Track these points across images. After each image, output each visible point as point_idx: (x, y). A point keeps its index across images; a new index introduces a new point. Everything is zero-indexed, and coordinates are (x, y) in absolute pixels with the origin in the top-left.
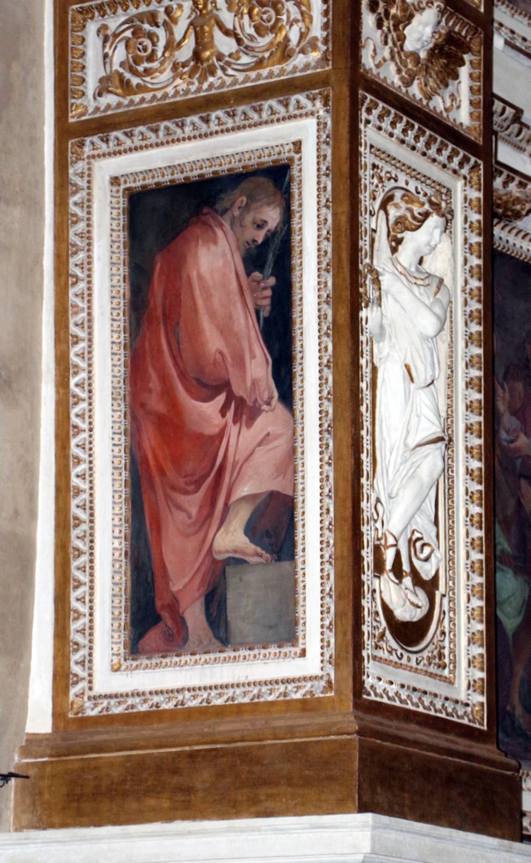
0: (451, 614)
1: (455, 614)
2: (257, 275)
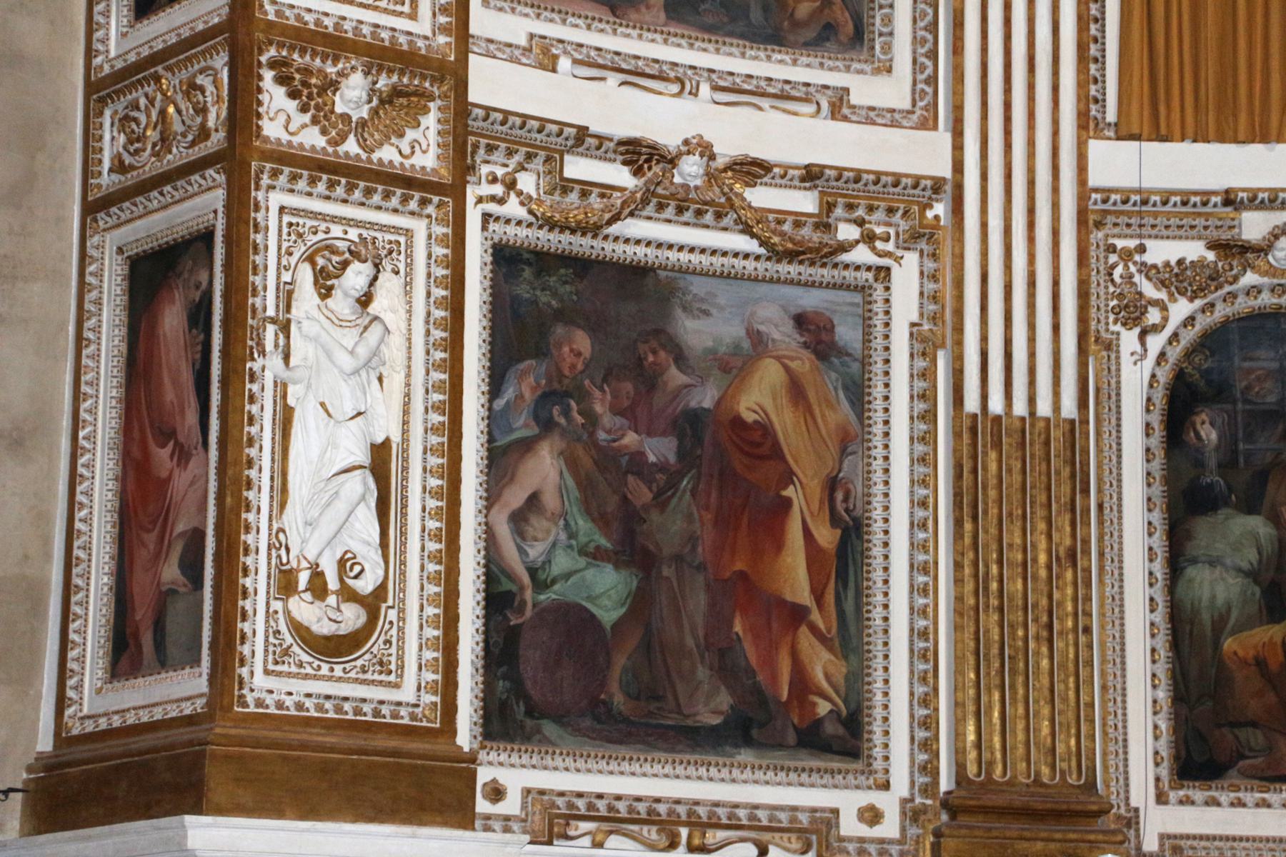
2: (194, 331)
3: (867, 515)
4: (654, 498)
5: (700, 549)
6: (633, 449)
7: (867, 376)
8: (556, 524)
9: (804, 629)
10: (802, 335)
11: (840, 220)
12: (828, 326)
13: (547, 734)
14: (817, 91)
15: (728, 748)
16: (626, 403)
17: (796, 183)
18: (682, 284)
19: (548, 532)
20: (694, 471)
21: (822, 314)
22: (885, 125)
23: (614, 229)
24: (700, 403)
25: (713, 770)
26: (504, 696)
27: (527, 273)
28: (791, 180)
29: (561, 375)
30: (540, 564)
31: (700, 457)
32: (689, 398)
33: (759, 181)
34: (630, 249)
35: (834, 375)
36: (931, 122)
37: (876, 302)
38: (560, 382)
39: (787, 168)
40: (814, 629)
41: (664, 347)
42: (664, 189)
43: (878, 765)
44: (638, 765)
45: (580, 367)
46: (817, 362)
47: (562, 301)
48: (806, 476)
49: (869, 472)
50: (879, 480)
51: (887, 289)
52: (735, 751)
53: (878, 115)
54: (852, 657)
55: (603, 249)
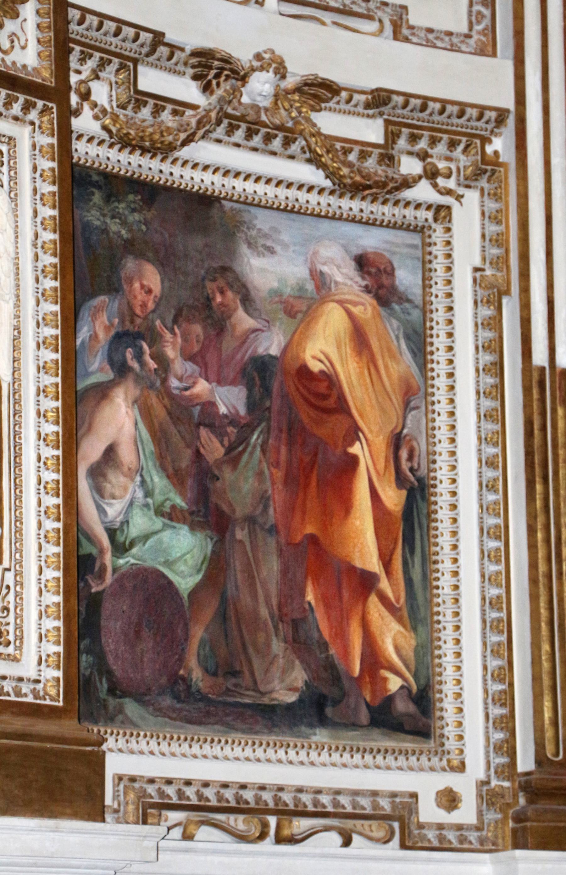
0: (18, 588)
1: (22, 588)
3: (432, 474)
4: (227, 453)
5: (271, 511)
6: (205, 398)
7: (428, 324)
8: (132, 480)
9: (373, 600)
10: (363, 279)
11: (402, 153)
12: (389, 269)
13: (129, 714)
14: (378, 8)
15: (303, 728)
16: (196, 349)
17: (360, 109)
18: (246, 217)
19: (125, 489)
20: (263, 425)
21: (381, 255)
22: (445, 49)
23: (185, 153)
24: (267, 349)
25: (292, 753)
26: (87, 673)
27: (97, 198)
28: (356, 106)
29: (133, 315)
30: (118, 524)
31: (269, 409)
32: (257, 343)
33: (323, 105)
34: (198, 175)
35: (395, 323)
36: (490, 49)
37: (435, 244)
38: (132, 322)
39: (352, 91)
40: (383, 598)
41: (231, 287)
42: (234, 109)
43: (451, 744)
44: (219, 748)
45: (151, 305)
46: (379, 309)
47: (130, 231)
48: (371, 432)
49: (434, 428)
50: (443, 438)
51: (448, 230)
52: (311, 731)
53: (437, 38)
54: (420, 629)
55: (171, 174)
